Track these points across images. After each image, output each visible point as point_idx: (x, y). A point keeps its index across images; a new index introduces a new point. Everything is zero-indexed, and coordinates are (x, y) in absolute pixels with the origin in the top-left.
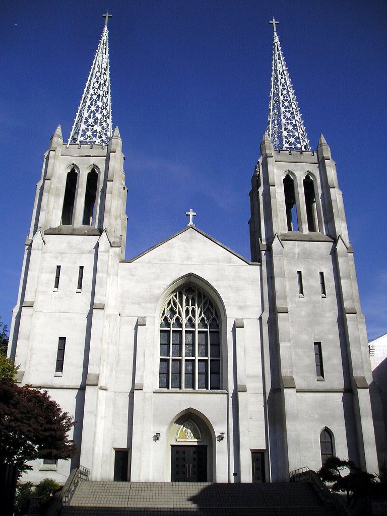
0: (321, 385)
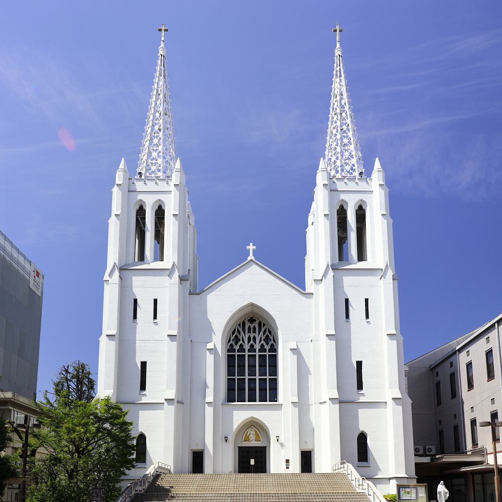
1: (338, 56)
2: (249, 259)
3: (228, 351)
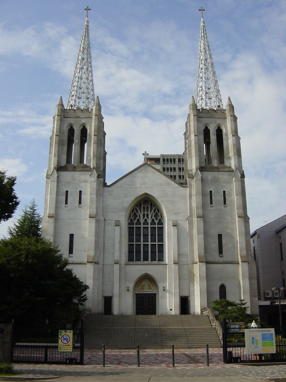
0: (221, 259)
1: (202, 27)
3: (129, 224)
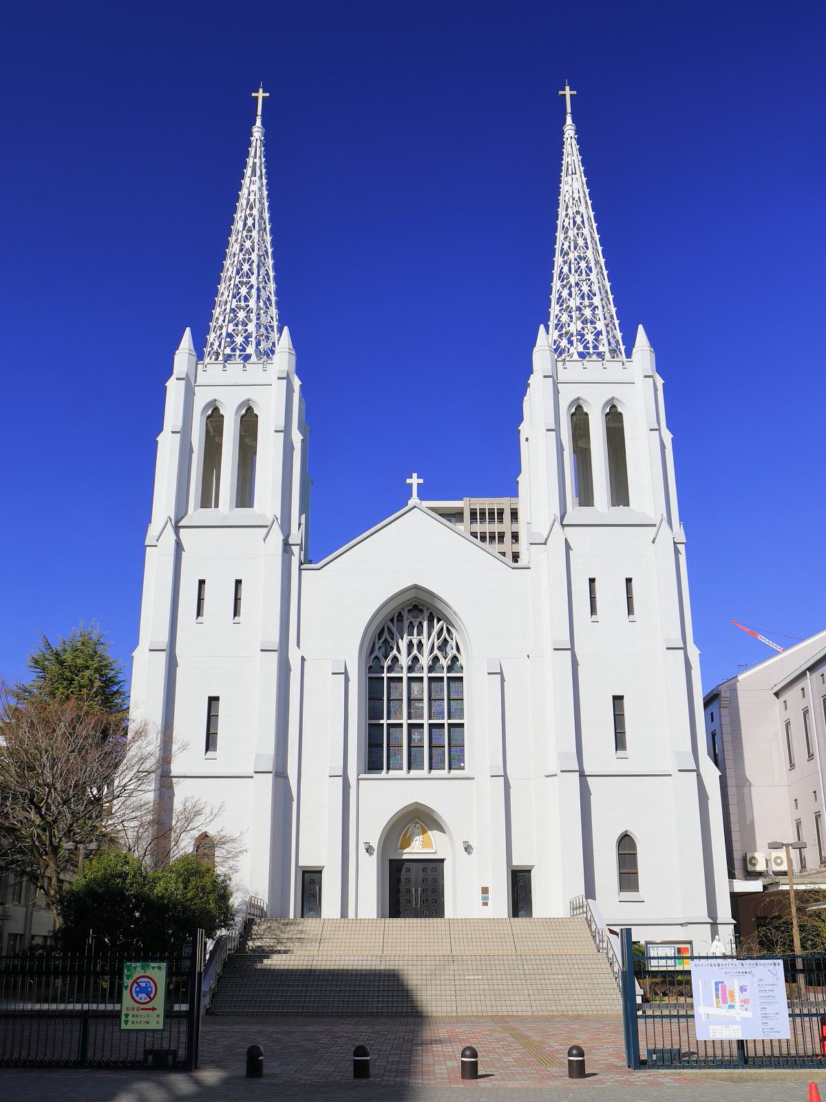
2: (411, 503)
